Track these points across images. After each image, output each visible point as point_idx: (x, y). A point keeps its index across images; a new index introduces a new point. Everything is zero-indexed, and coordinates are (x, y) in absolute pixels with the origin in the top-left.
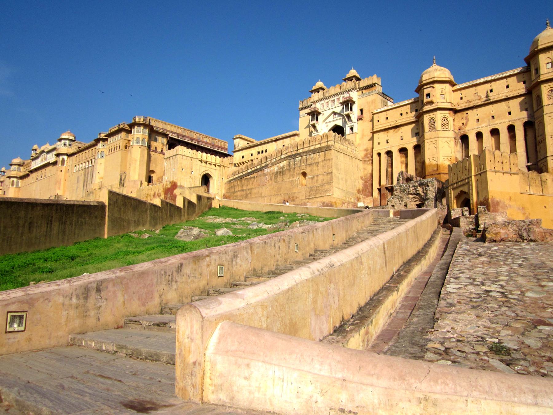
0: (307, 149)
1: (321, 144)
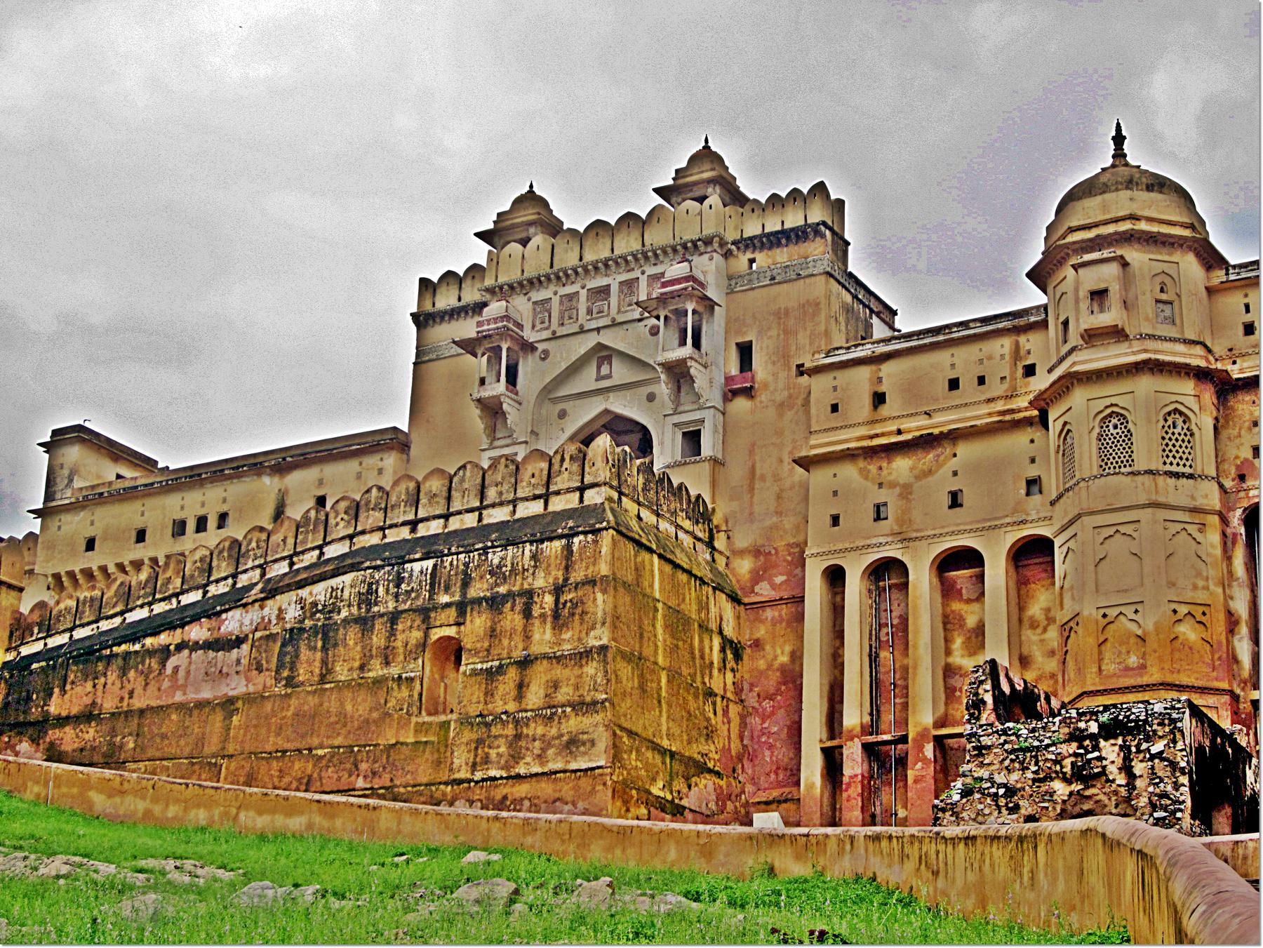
0: (470, 521)
1: (546, 497)
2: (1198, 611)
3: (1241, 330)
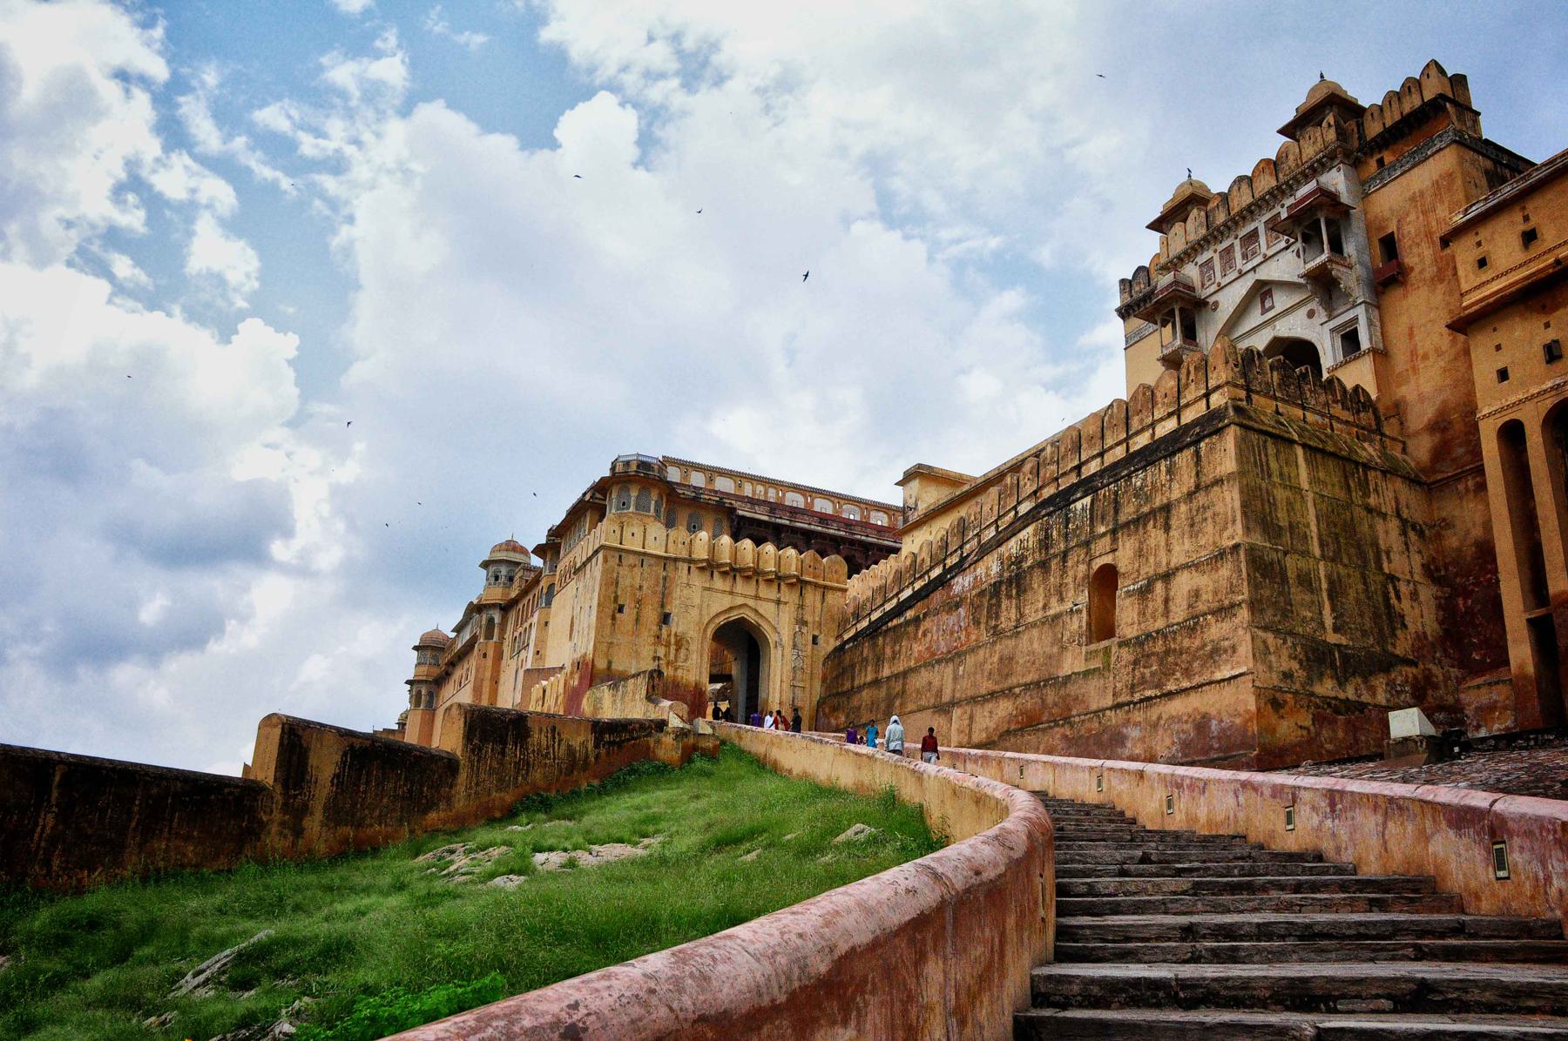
0: (1119, 453)
1: (1177, 413)
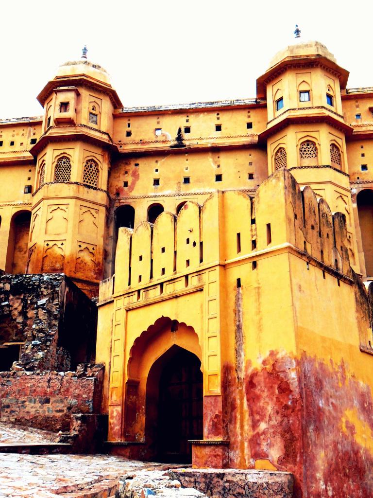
2: (91, 248)
3: (125, 134)
